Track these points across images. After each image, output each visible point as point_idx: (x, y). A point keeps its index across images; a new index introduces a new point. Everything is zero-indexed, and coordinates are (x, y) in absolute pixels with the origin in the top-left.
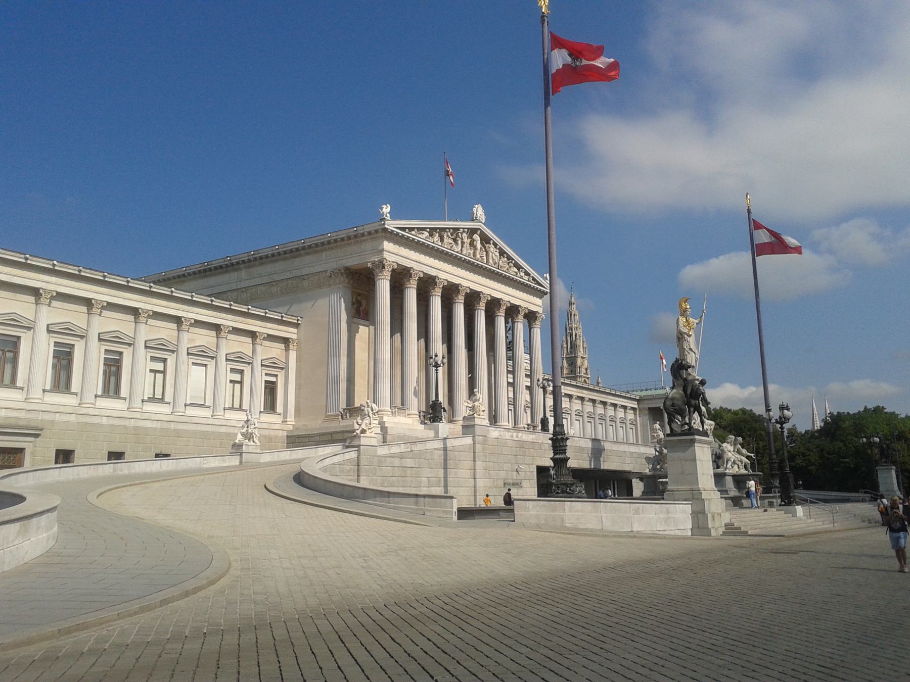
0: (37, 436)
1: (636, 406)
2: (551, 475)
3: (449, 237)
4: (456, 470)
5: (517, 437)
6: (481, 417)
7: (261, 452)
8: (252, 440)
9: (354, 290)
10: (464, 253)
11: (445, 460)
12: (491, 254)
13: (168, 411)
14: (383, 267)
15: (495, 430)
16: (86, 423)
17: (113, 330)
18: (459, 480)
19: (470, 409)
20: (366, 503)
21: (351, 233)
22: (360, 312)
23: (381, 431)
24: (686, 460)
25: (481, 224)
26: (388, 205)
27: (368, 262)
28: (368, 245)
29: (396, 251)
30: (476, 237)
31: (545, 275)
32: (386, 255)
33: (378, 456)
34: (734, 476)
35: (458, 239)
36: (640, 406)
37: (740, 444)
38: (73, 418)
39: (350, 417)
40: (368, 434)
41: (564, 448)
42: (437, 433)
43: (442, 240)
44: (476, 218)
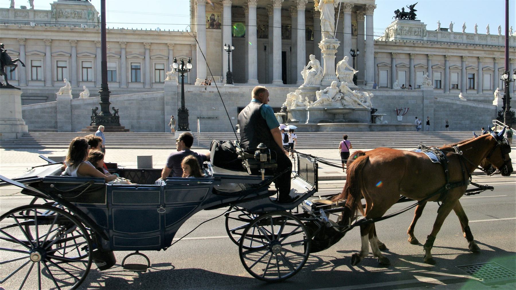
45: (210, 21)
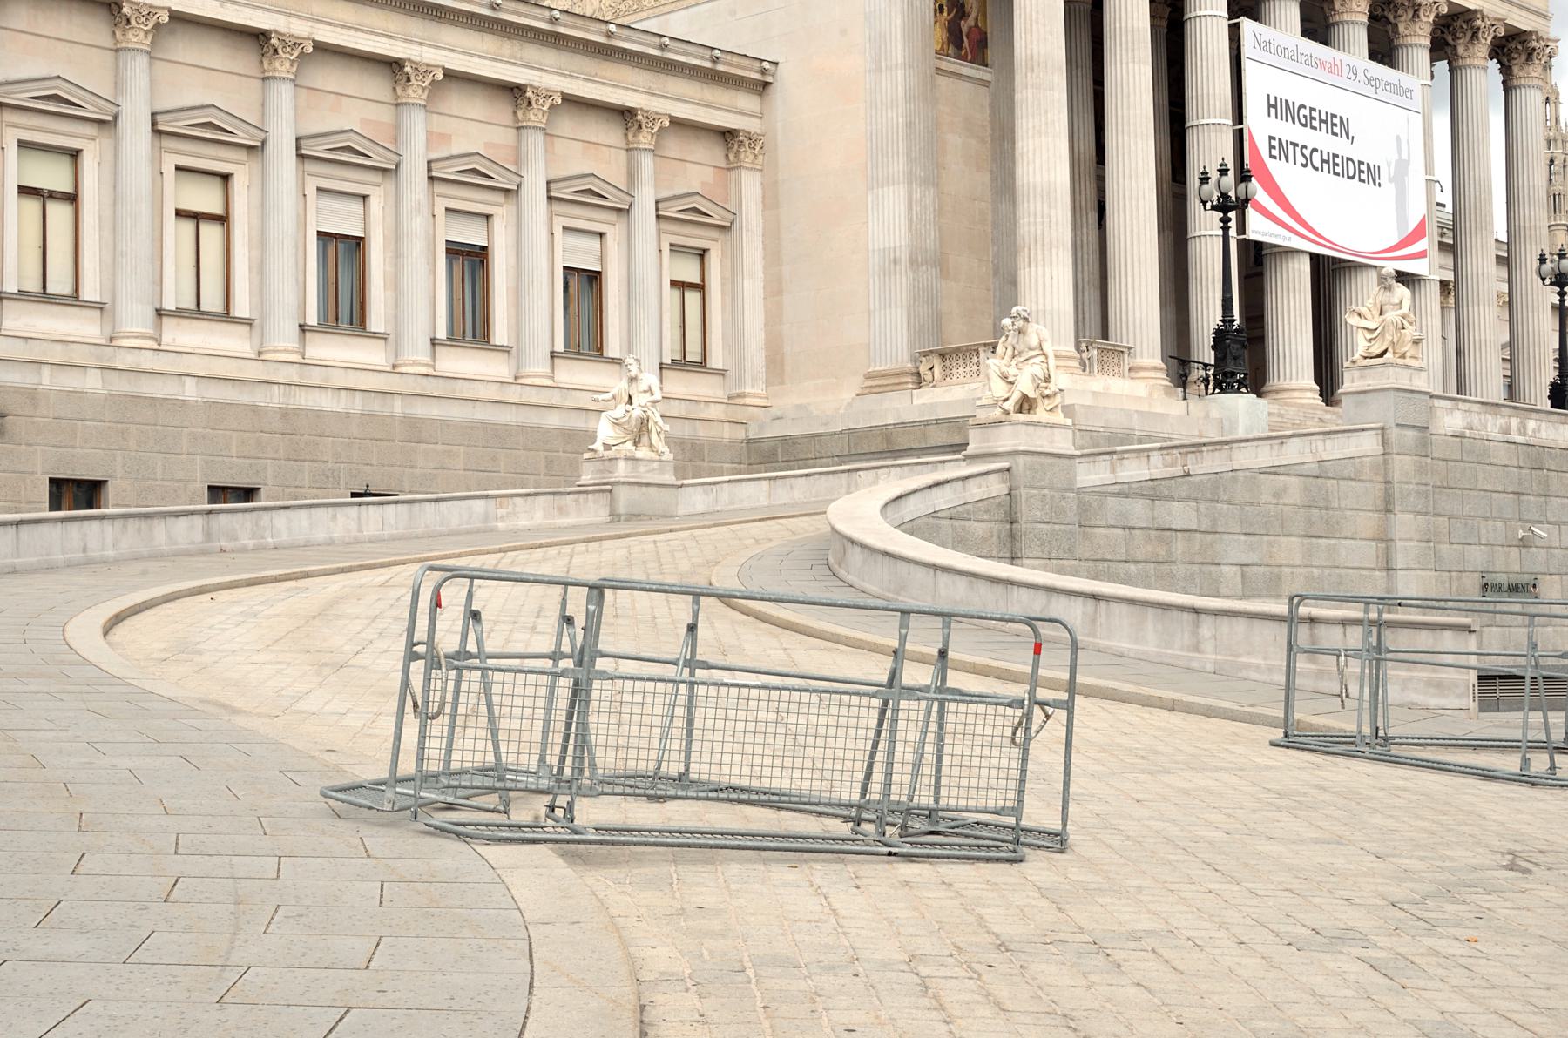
4: (1333, 541)
5: (1522, 430)
6: (1408, 361)
7: (679, 483)
8: (645, 439)
13: (384, 363)
15: (1452, 410)
16: (135, 398)
17: (198, 103)
18: (1340, 576)
19: (1369, 336)
22: (963, 41)
33: (1079, 491)
38: (93, 382)
39: (945, 377)
40: (1040, 414)
45: (945, 14)
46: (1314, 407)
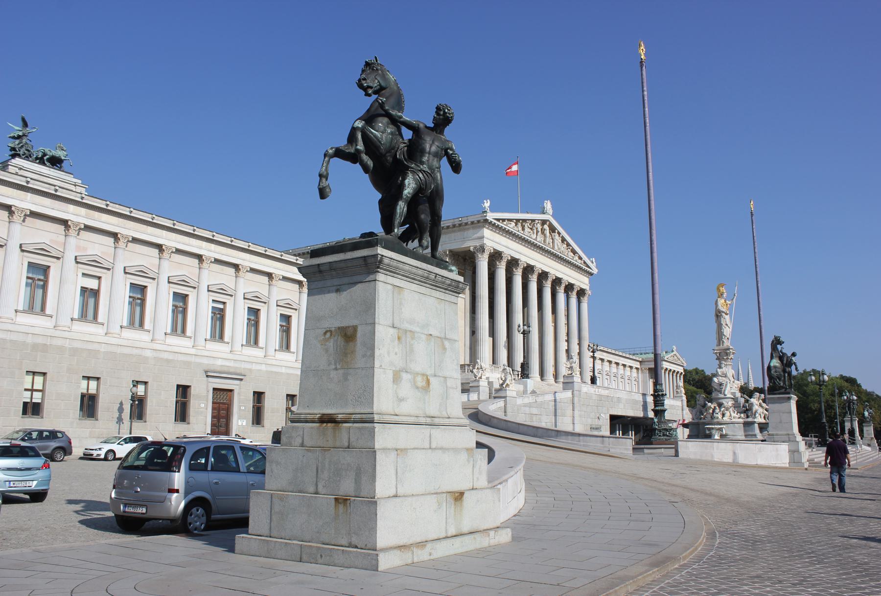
0: (241, 380)
1: (639, 367)
2: (655, 422)
3: (529, 227)
9: (460, 271)
10: (538, 240)
11: (555, 410)
12: (556, 241)
14: (484, 251)
17: (285, 298)
20: (558, 441)
21: (457, 222)
23: (488, 384)
24: (783, 413)
25: (550, 216)
26: (488, 201)
27: (470, 246)
28: (470, 233)
29: (492, 238)
30: (546, 227)
31: (591, 259)
32: (486, 241)
34: (759, 424)
35: (534, 228)
36: (642, 366)
37: (762, 400)
40: (510, 388)
41: (662, 402)
42: (526, 387)
43: (523, 229)
44: (546, 211)
46: (539, 382)
